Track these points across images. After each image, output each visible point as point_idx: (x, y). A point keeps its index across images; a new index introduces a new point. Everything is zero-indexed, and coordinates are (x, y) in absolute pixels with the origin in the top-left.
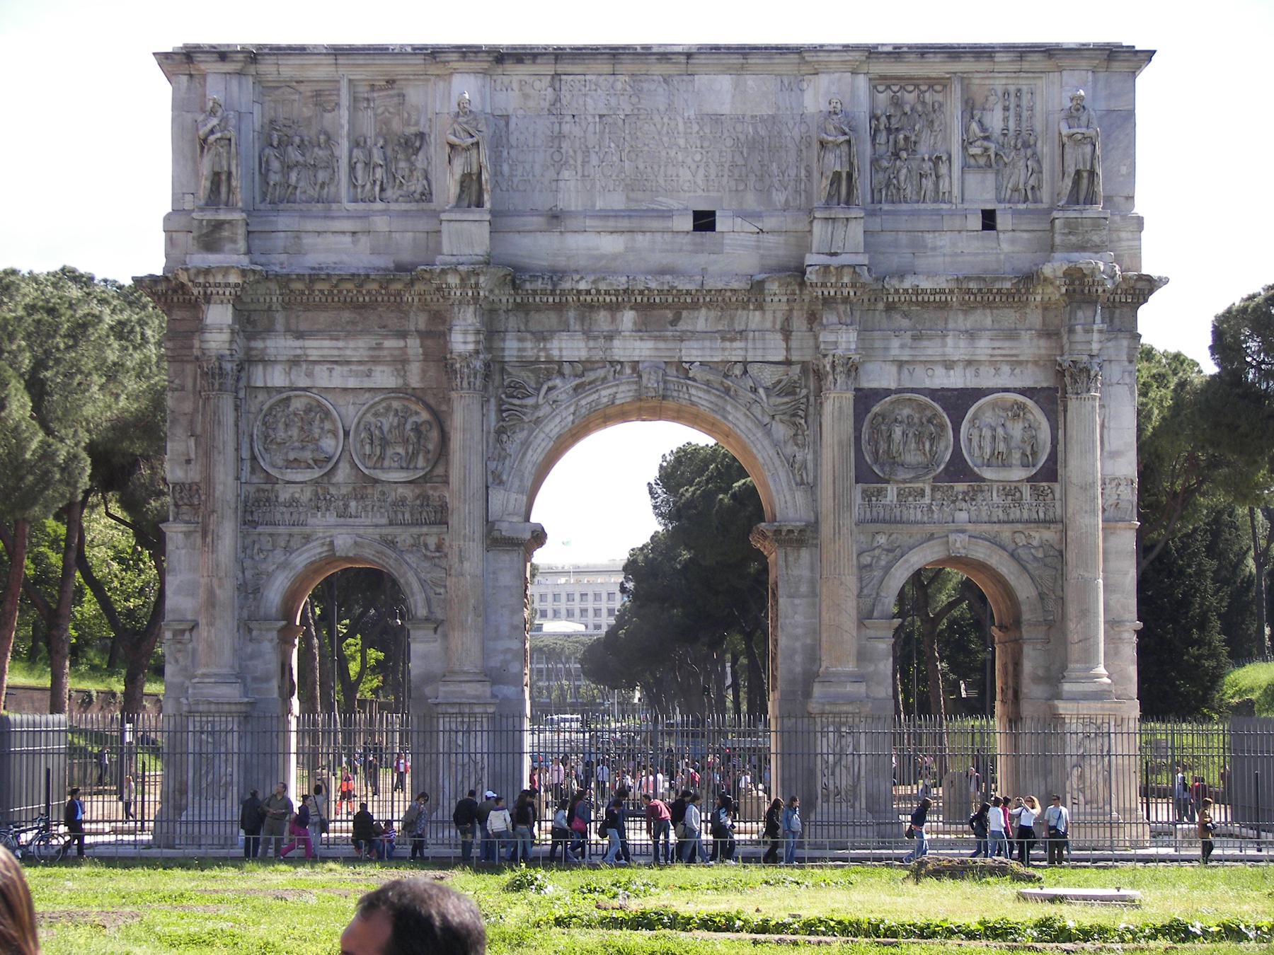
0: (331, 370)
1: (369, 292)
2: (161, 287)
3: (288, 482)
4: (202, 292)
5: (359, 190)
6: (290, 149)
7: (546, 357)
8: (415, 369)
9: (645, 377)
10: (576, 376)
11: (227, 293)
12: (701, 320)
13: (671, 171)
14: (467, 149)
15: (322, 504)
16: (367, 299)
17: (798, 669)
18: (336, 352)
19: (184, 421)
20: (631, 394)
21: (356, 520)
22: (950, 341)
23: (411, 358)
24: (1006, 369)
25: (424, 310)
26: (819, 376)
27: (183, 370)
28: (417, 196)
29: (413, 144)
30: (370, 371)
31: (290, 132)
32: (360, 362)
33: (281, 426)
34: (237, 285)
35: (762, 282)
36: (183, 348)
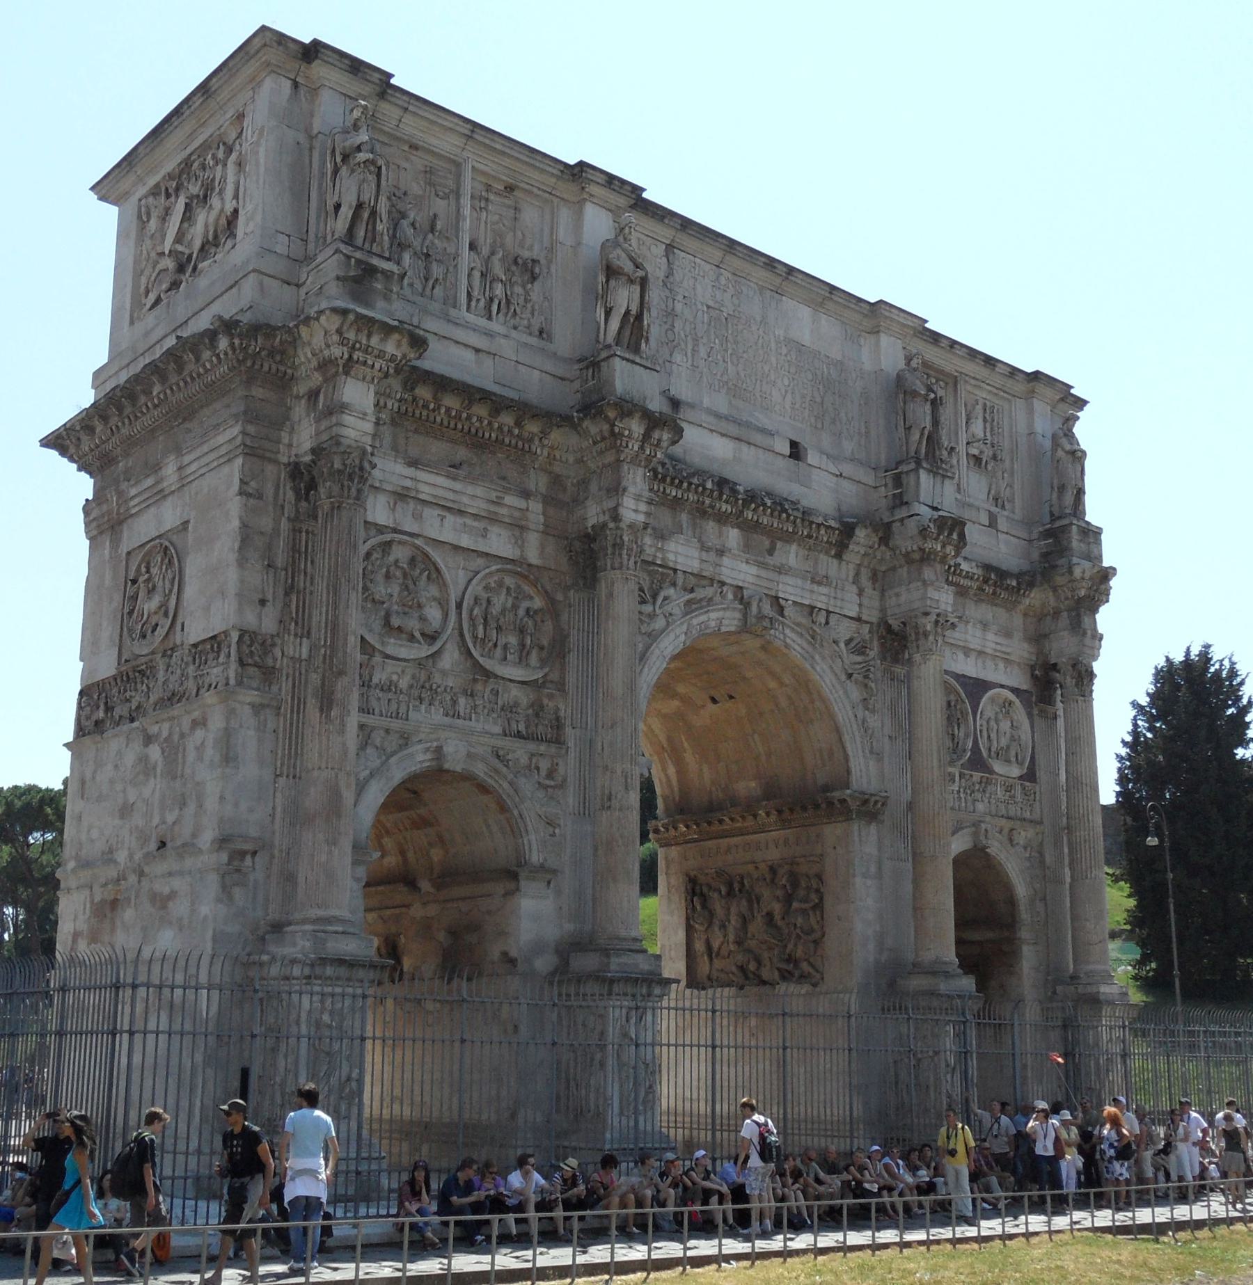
0: (443, 518)
1: (500, 428)
3: (388, 656)
4: (346, 356)
5: (473, 303)
6: (405, 223)
7: (663, 559)
8: (533, 539)
9: (754, 609)
10: (685, 590)
11: (377, 366)
12: (791, 555)
16: (493, 435)
18: (451, 496)
20: (735, 622)
21: (467, 723)
22: (970, 626)
23: (532, 526)
24: (1001, 665)
25: (545, 471)
30: (485, 529)
31: (400, 206)
32: (475, 516)
33: (380, 577)
34: (393, 358)
36: (268, 439)
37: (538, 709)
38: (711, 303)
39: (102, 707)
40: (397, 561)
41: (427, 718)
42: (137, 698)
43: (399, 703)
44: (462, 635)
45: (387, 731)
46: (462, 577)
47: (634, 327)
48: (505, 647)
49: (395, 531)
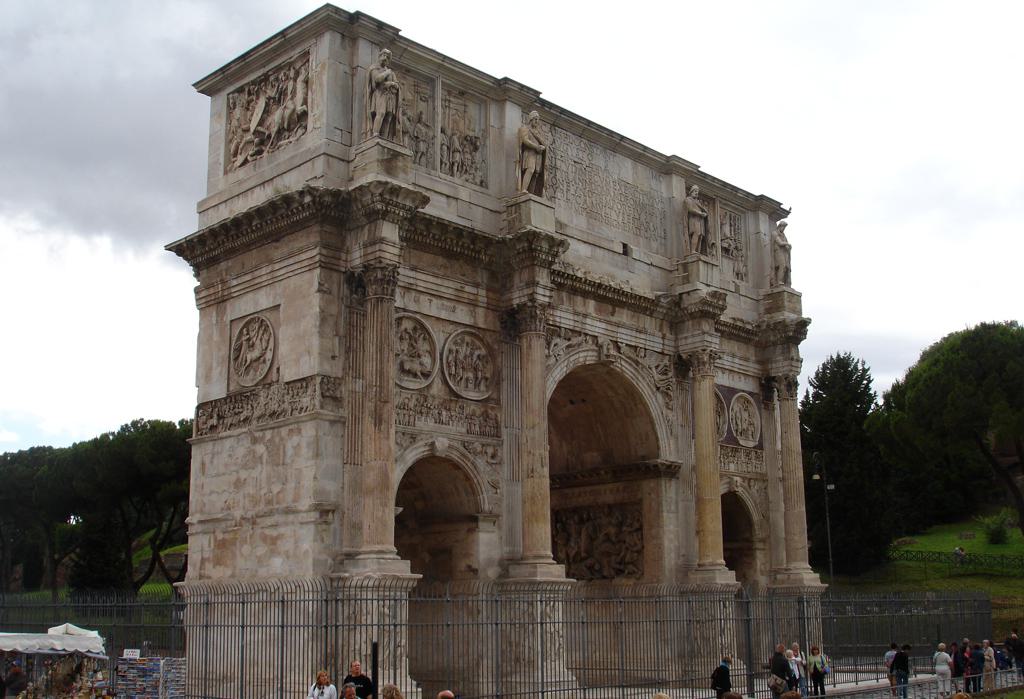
0: (431, 301)
2: (328, 199)
3: (402, 388)
8: (481, 312)
9: (605, 351)
12: (623, 316)
13: (608, 211)
14: (536, 152)
15: (424, 410)
17: (673, 563)
18: (434, 287)
19: (331, 321)
24: (743, 378)
26: (684, 367)
27: (331, 277)
28: (478, 181)
29: (473, 144)
34: (410, 209)
35: (660, 296)
37: (485, 416)
38: (576, 160)
39: (215, 416)
40: (406, 330)
41: (425, 424)
42: (245, 412)
43: (410, 416)
44: (443, 373)
45: (403, 434)
46: (442, 337)
47: (538, 184)
48: (467, 379)
49: (405, 310)
